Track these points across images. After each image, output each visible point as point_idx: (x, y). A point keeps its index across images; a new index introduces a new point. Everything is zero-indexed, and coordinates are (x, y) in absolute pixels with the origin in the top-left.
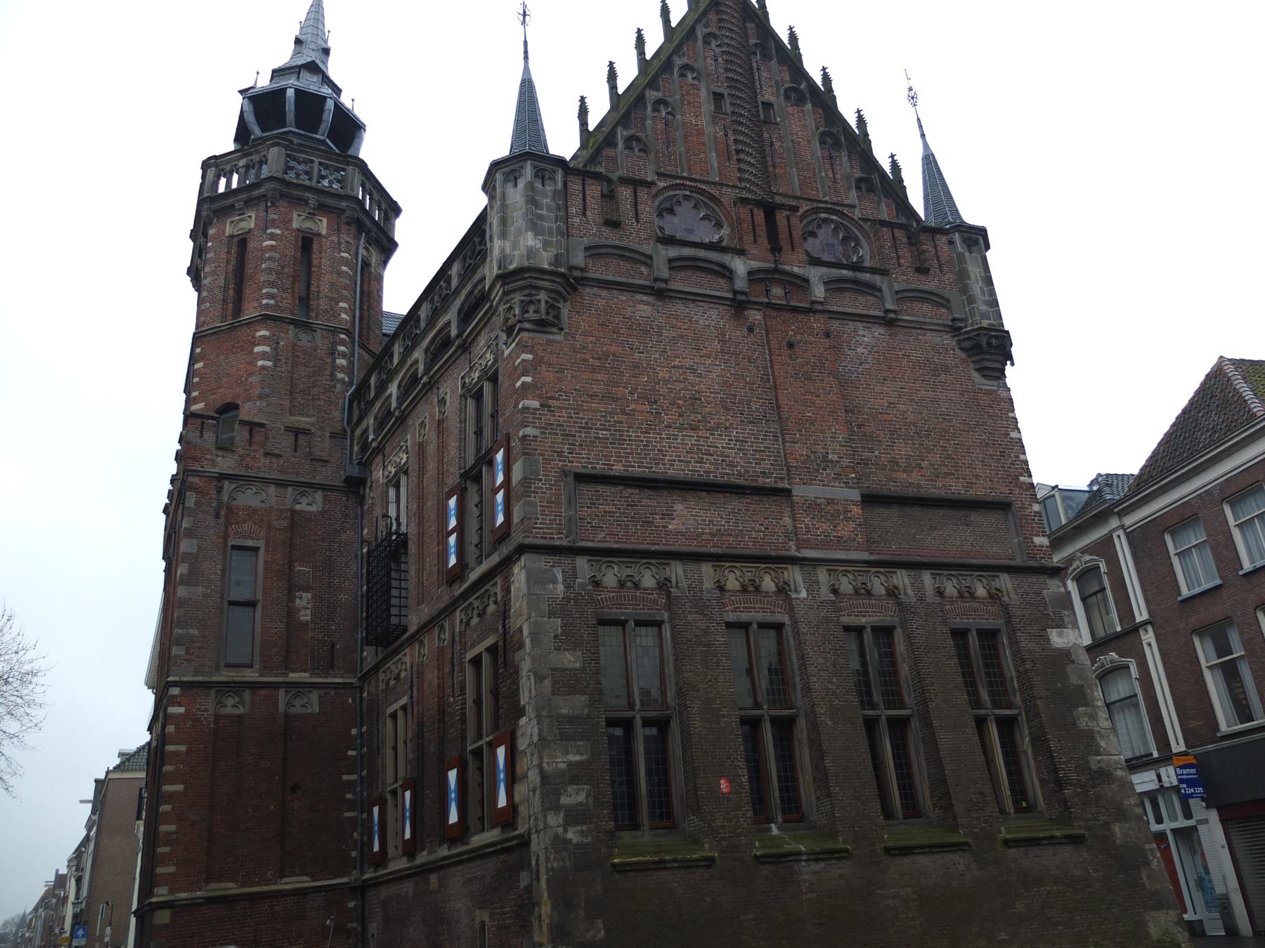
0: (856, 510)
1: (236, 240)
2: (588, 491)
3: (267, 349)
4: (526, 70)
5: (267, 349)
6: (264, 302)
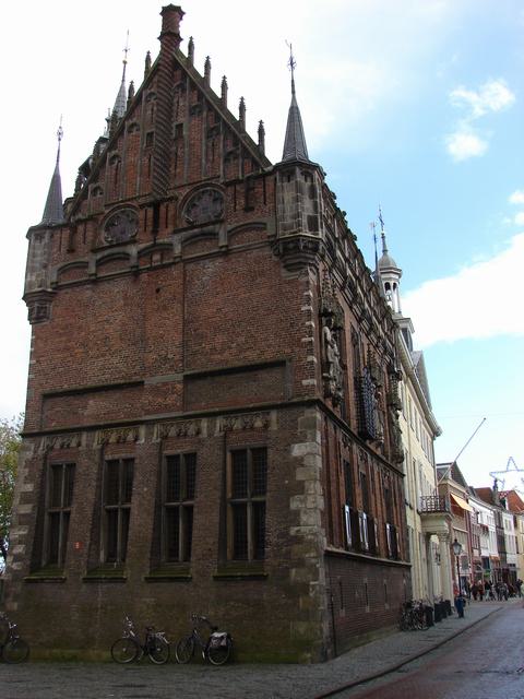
0: (179, 386)
2: (49, 403)
4: (57, 169)
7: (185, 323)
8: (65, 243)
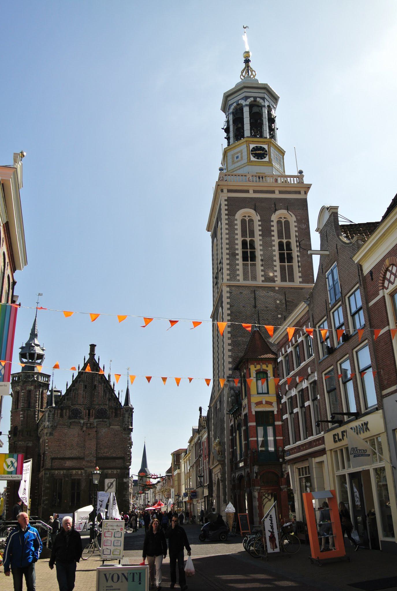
7: (97, 444)
8: (59, 414)
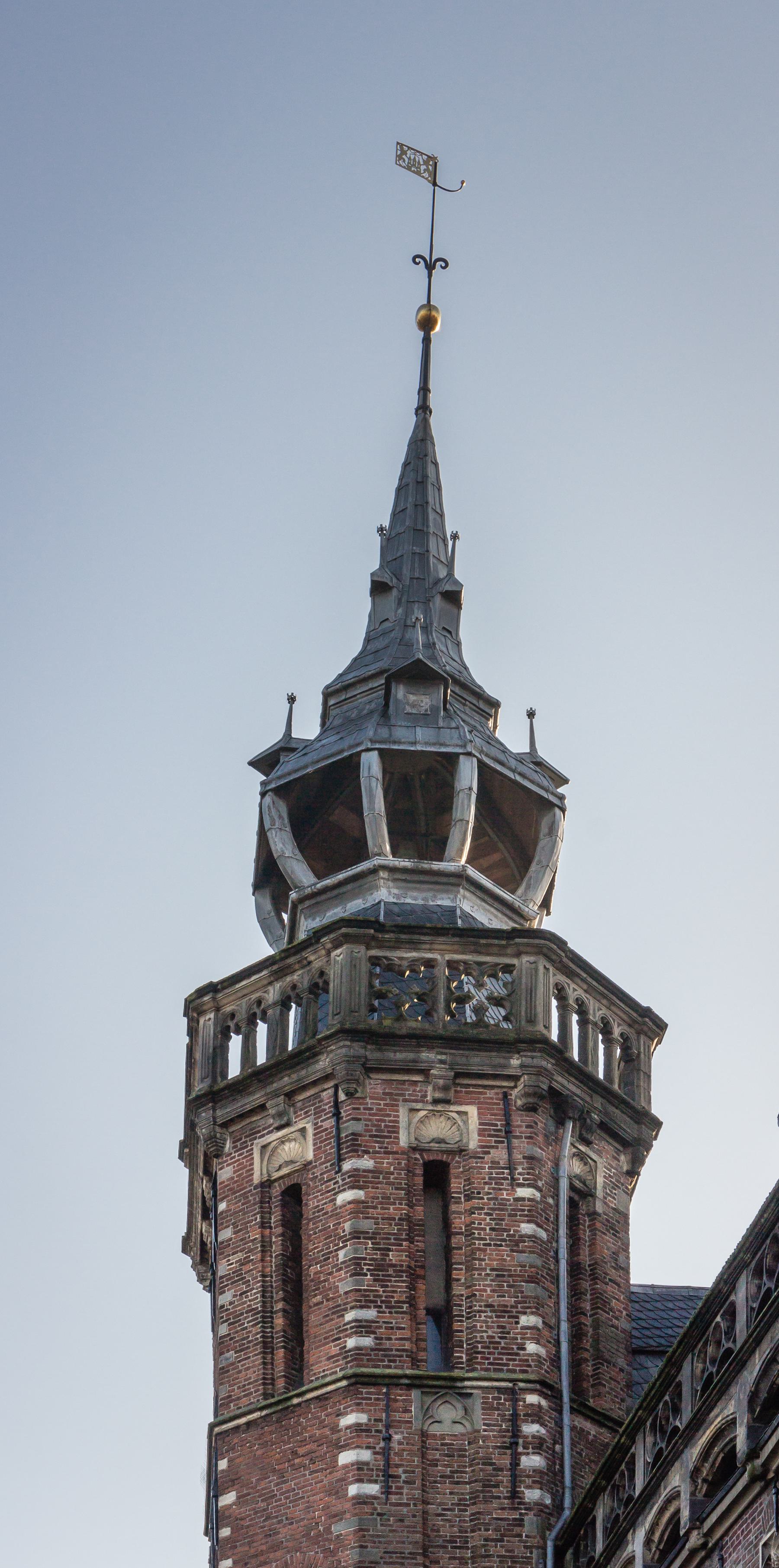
1: (276, 1190)
3: (366, 1455)
5: (366, 1455)
6: (351, 1343)
